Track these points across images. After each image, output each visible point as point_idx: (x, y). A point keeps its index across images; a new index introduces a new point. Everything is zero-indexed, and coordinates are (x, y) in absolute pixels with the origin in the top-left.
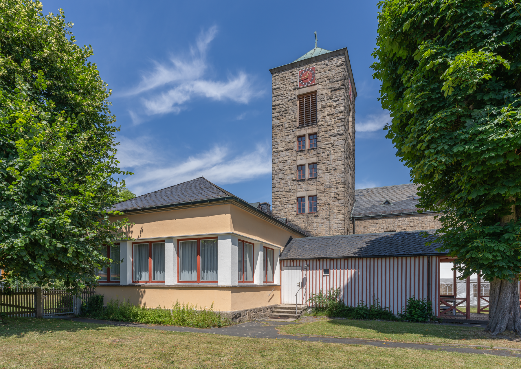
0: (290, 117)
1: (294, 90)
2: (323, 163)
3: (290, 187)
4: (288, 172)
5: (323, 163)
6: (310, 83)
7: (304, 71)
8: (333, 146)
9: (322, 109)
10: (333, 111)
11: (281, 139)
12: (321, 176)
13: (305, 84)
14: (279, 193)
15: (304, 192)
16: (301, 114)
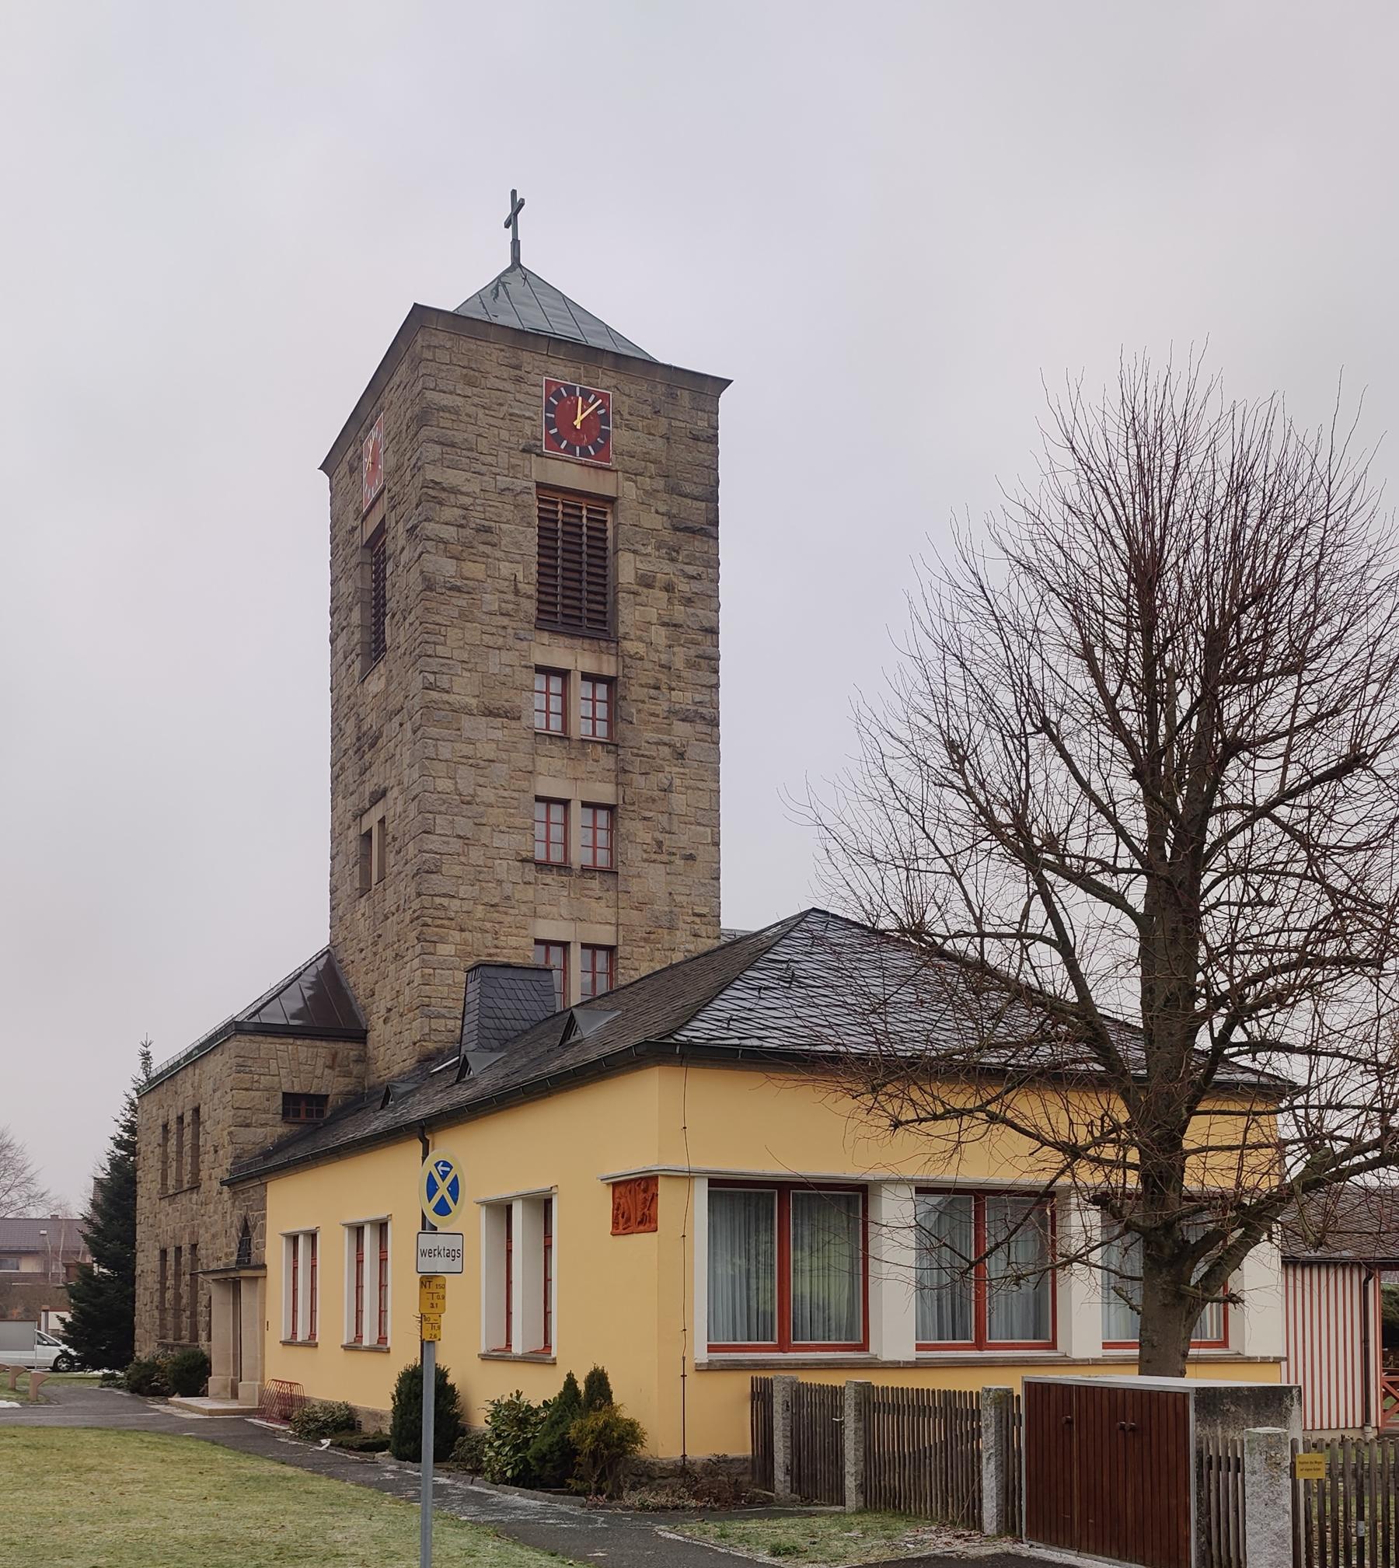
0: (506, 569)
1: (524, 451)
2: (645, 819)
3: (508, 888)
4: (496, 816)
5: (645, 819)
6: (587, 455)
7: (566, 387)
8: (681, 756)
9: (640, 589)
10: (679, 612)
11: (465, 657)
12: (633, 871)
13: (570, 449)
14: (457, 902)
15: (563, 924)
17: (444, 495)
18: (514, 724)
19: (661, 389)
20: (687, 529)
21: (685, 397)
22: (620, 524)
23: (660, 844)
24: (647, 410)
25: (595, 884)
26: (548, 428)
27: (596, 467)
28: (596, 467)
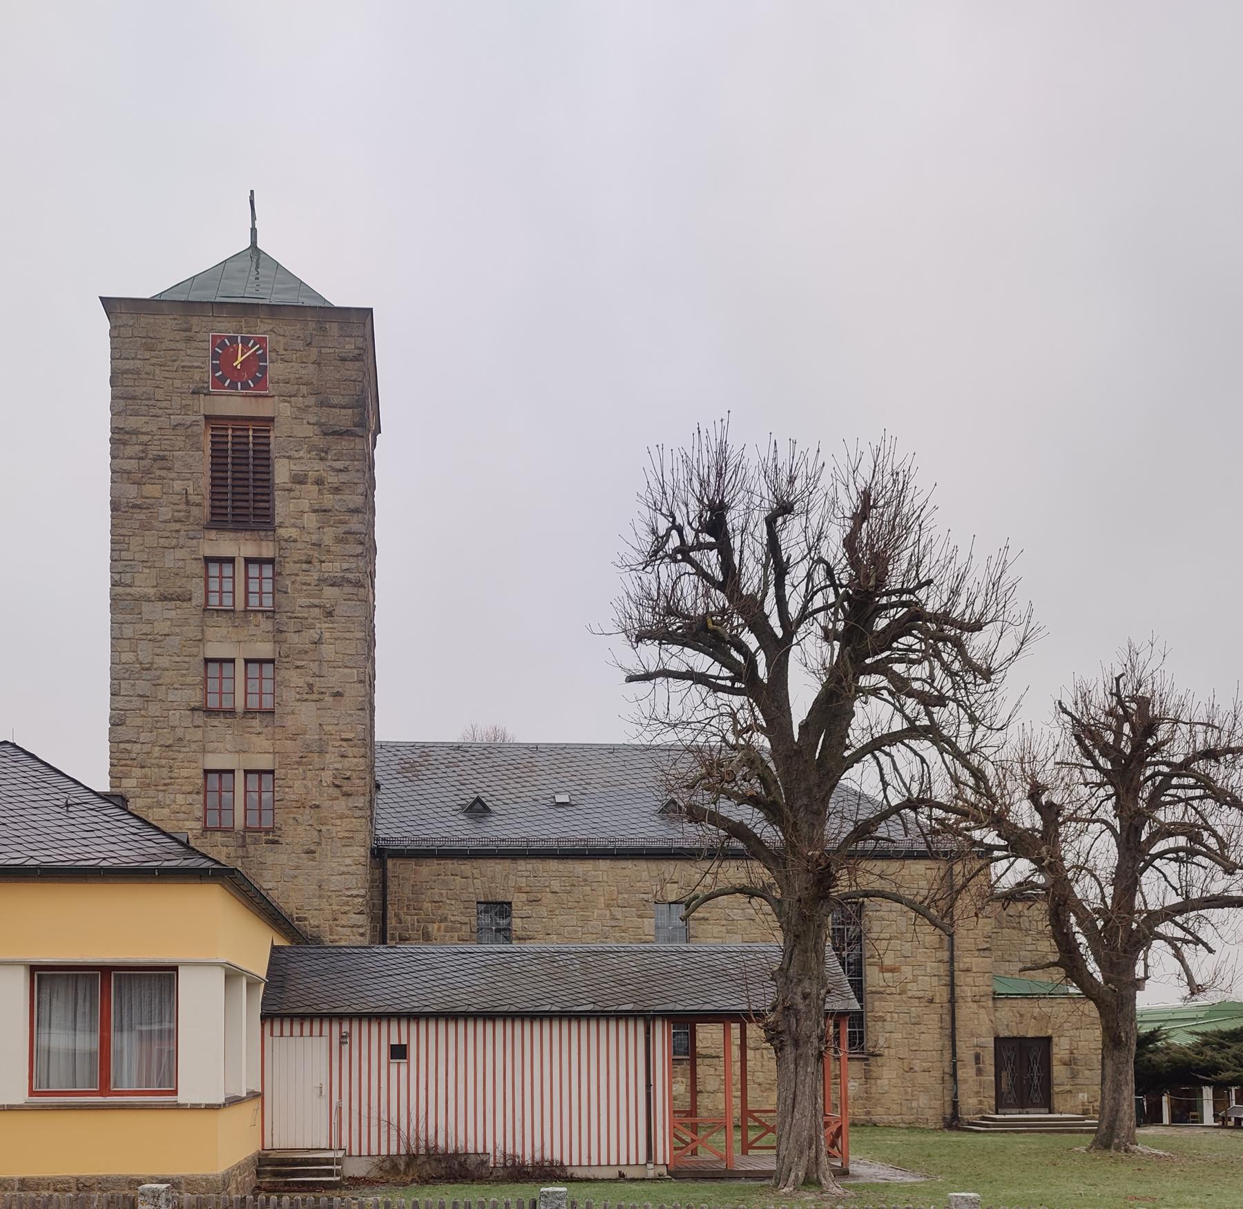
0: (178, 486)
1: (193, 393)
2: (298, 667)
3: (179, 732)
4: (168, 677)
5: (298, 667)
6: (249, 388)
7: (229, 338)
8: (330, 614)
9: (293, 486)
10: (329, 500)
11: (145, 557)
12: (288, 709)
13: (231, 386)
14: (139, 746)
15: (228, 756)
16: (217, 482)
17: (127, 437)
18: (185, 605)
19: (312, 325)
20: (334, 433)
21: (334, 329)
22: (276, 438)
23: (311, 686)
24: (299, 344)
25: (256, 723)
26: (214, 372)
27: (255, 396)
28: (255, 396)
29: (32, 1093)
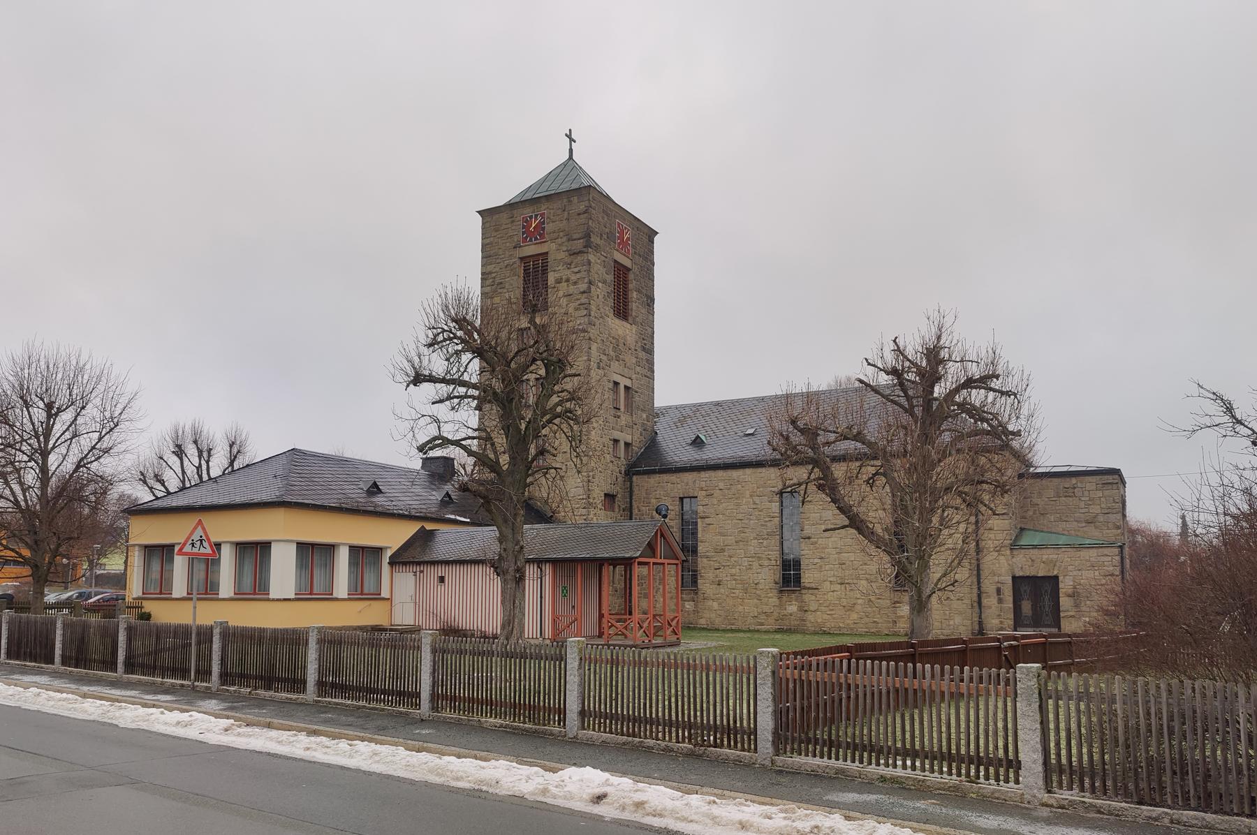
1: (514, 248)
6: (537, 239)
10: (572, 289)
13: (531, 240)
19: (565, 200)
20: (574, 254)
24: (559, 212)
26: (523, 234)
27: (541, 243)
28: (541, 243)
29: (235, 594)
